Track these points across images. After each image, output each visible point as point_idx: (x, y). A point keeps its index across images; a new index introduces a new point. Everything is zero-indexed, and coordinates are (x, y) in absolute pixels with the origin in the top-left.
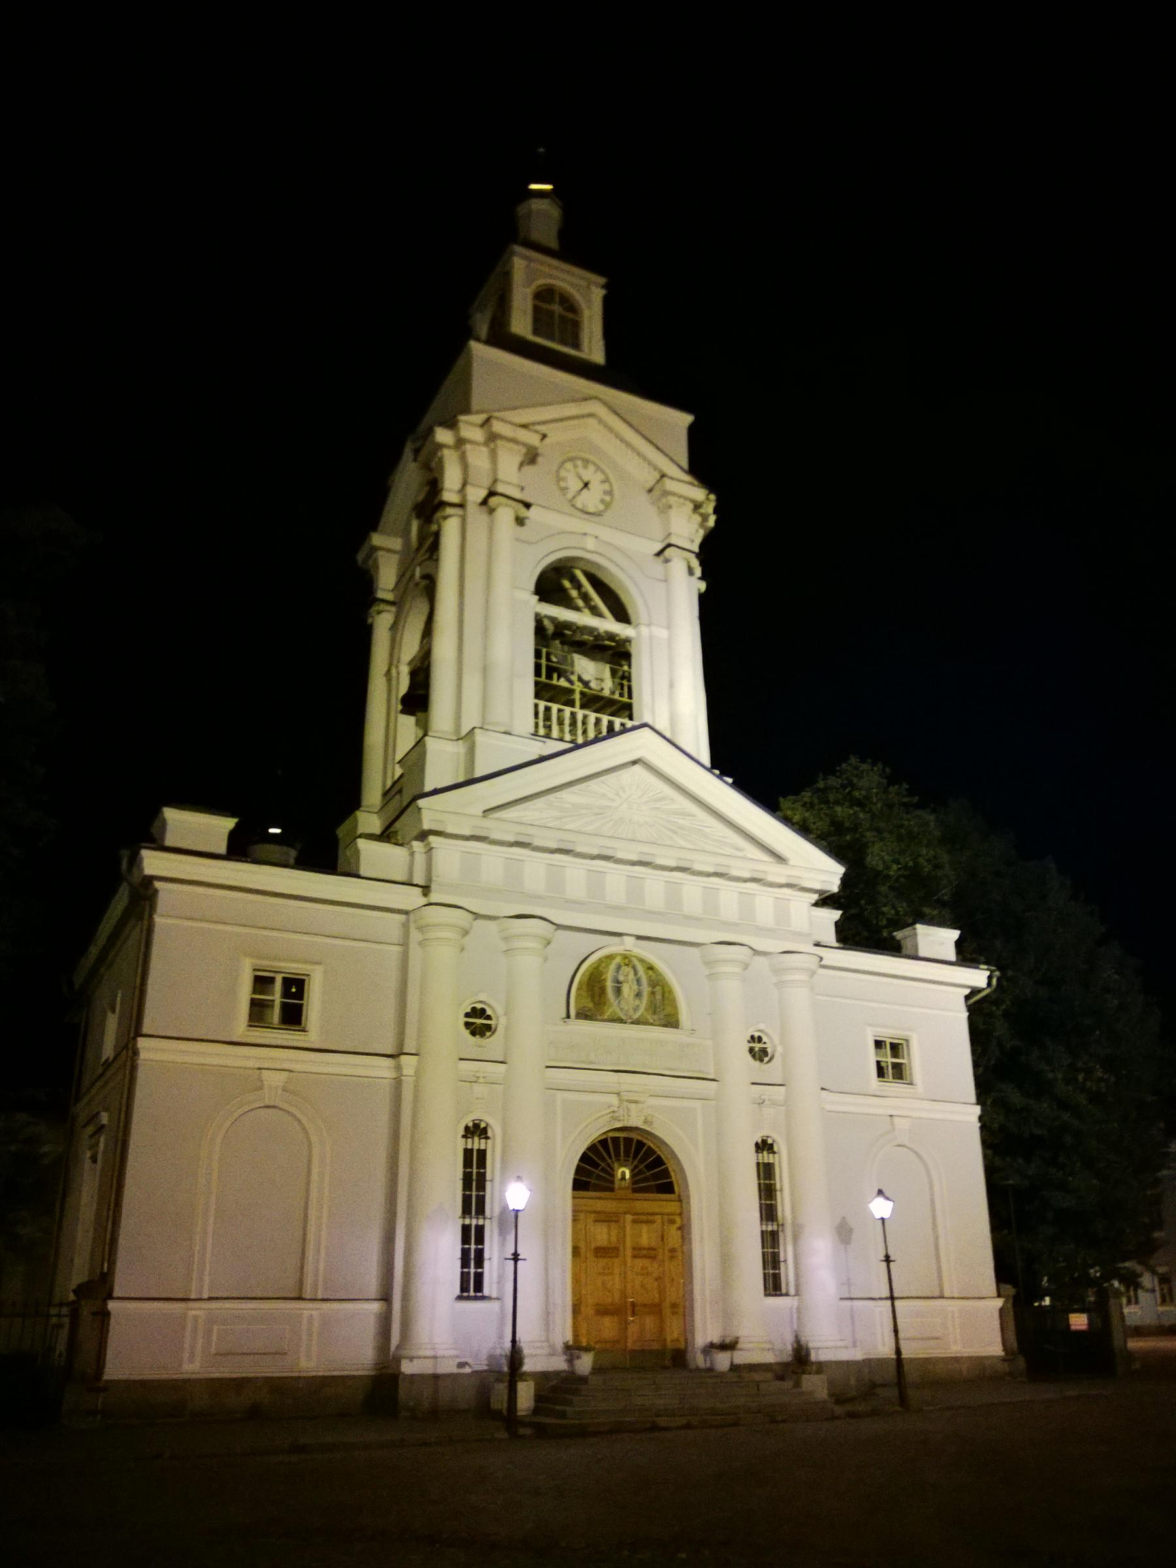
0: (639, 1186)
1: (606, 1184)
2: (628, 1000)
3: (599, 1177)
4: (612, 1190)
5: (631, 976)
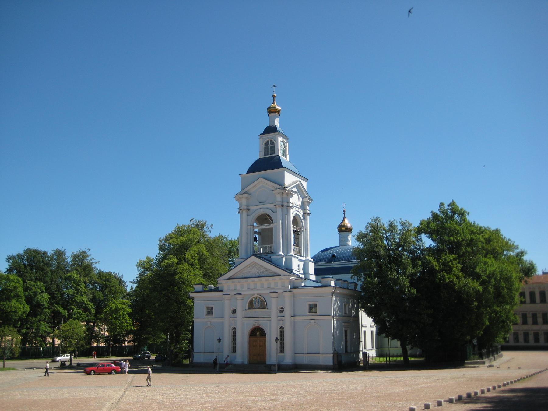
1: (255, 335)
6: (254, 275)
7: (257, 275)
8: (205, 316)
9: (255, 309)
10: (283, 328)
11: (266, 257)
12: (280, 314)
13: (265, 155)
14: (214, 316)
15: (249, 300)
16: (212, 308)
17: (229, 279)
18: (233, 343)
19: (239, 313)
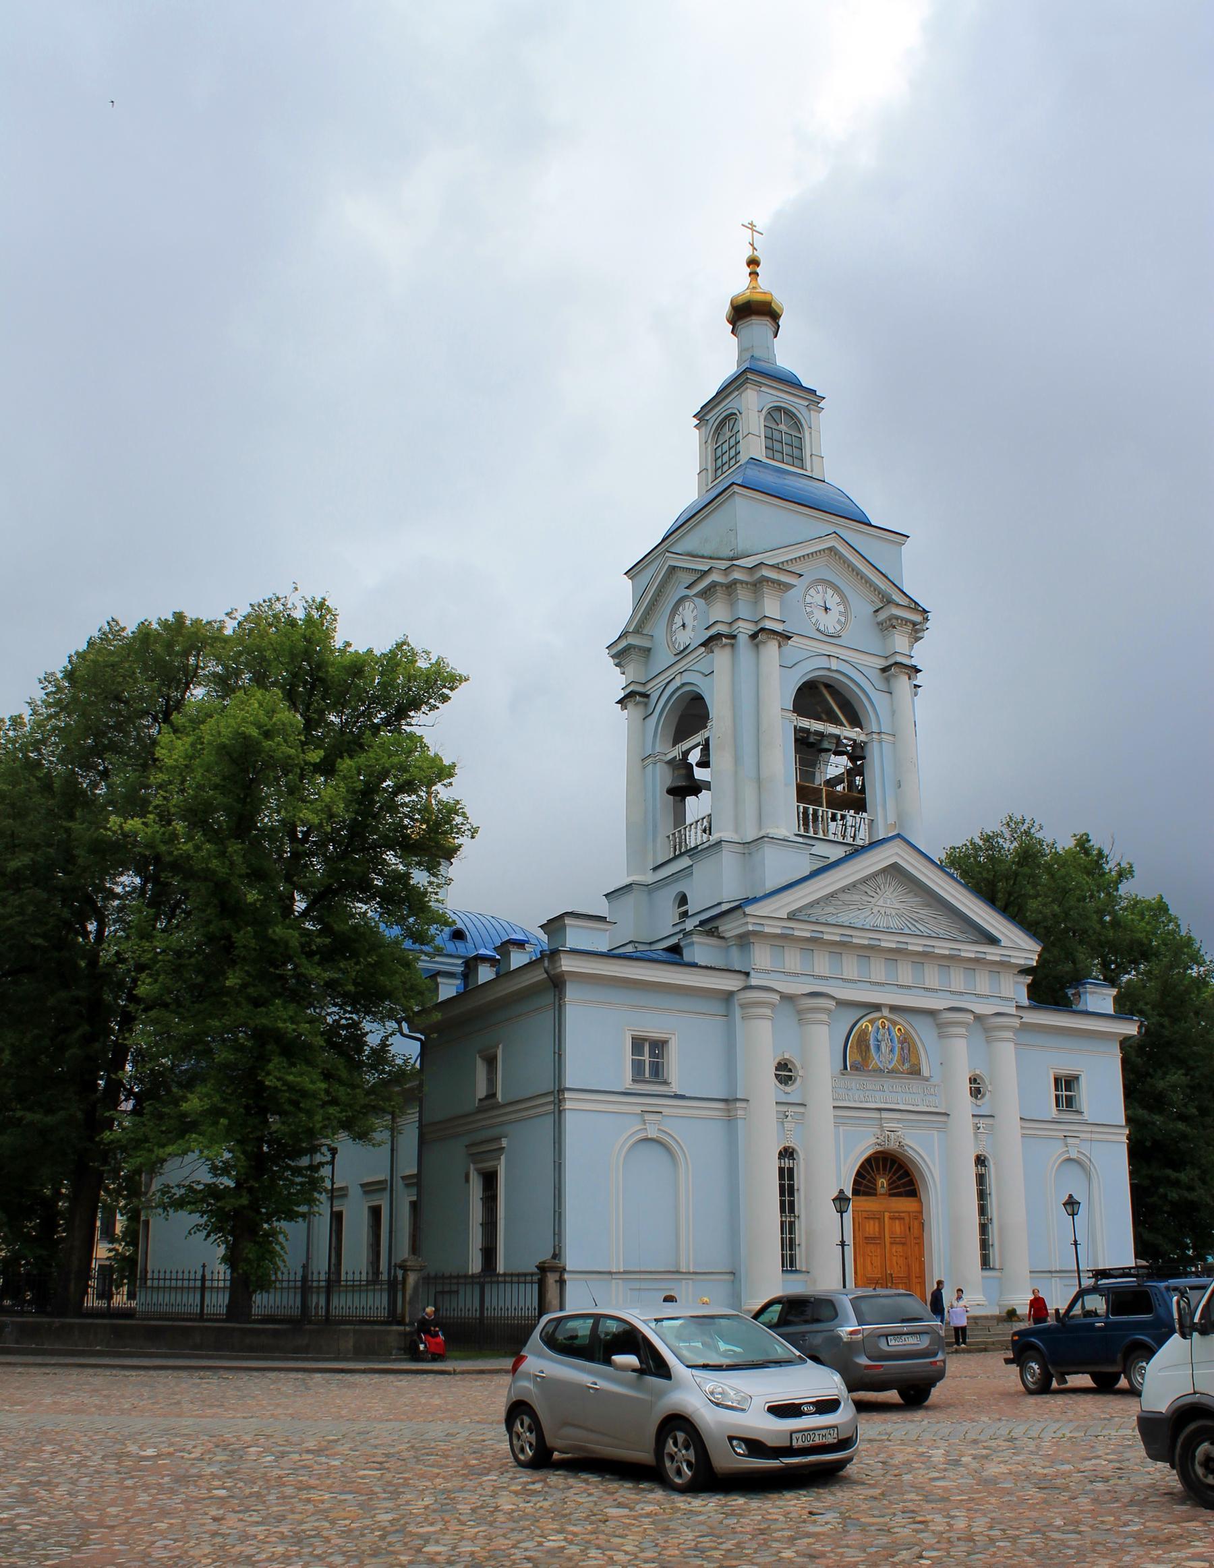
0: (894, 1192)
2: (884, 1057)
3: (866, 1186)
4: (875, 1195)
5: (887, 1035)
6: (882, 923)
7: (894, 923)
17: (792, 917)
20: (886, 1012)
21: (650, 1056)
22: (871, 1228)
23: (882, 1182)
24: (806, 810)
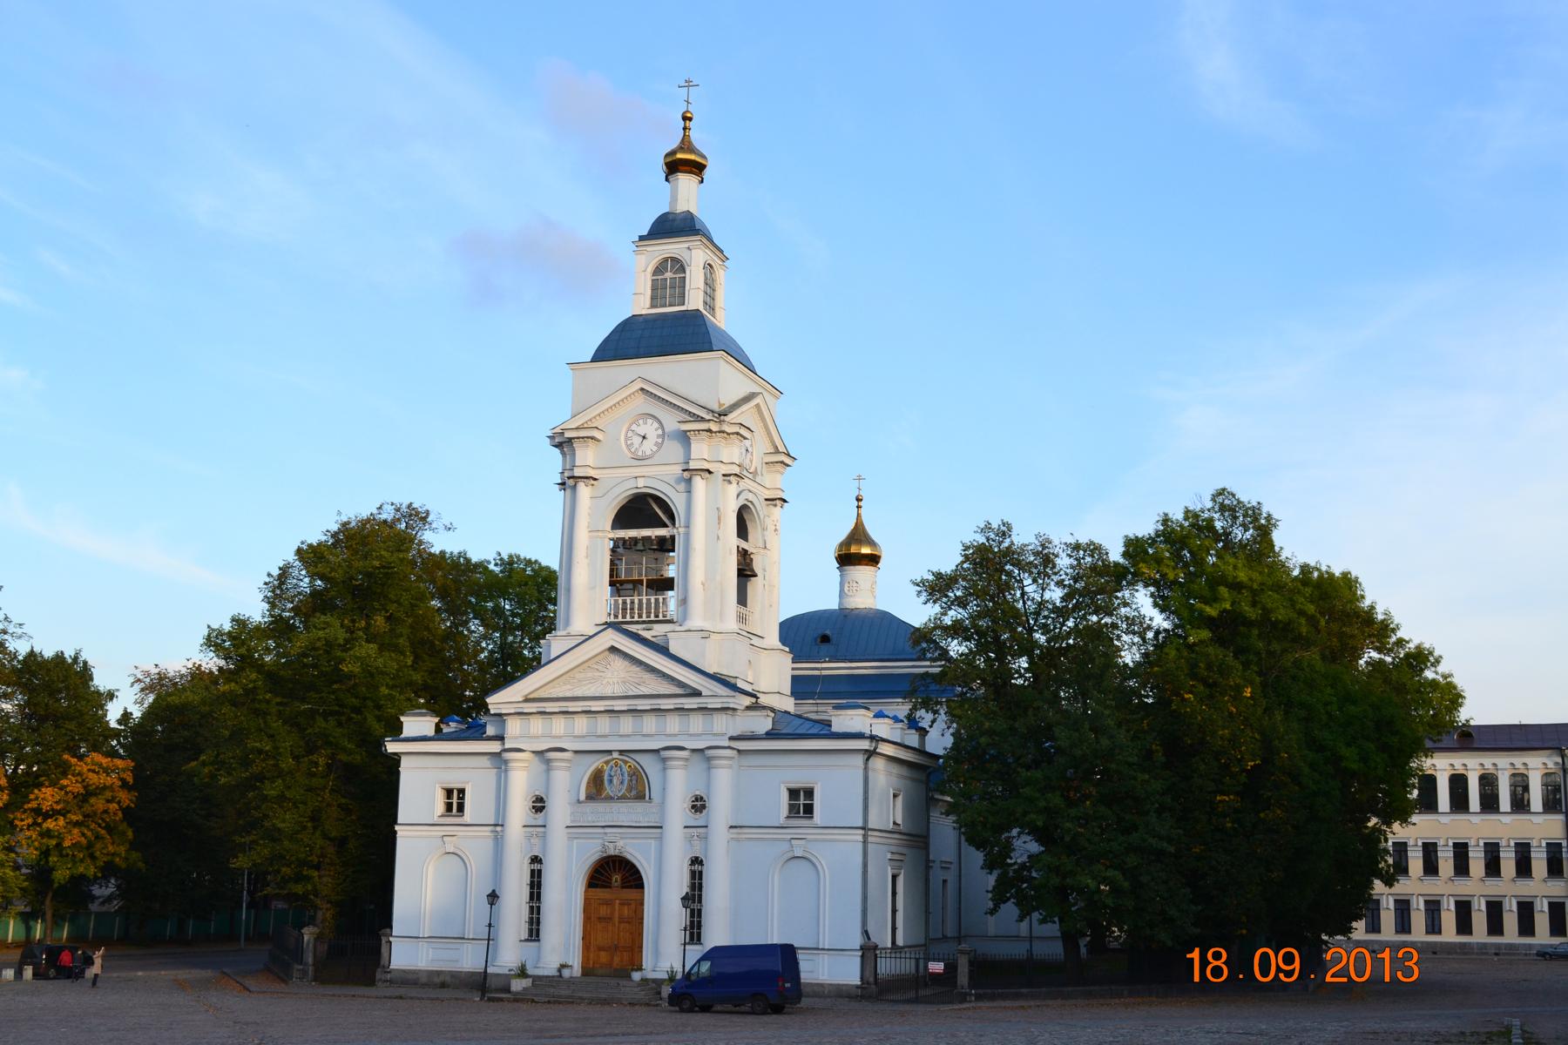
7: (619, 691)
8: (436, 820)
9: (610, 798)
10: (701, 863)
11: (647, 635)
12: (693, 819)
13: (653, 306)
14: (468, 816)
15: (592, 769)
16: (462, 791)
18: (532, 908)
19: (560, 811)
20: (615, 755)
21: (455, 800)
22: (604, 911)
23: (616, 878)
24: (624, 603)
